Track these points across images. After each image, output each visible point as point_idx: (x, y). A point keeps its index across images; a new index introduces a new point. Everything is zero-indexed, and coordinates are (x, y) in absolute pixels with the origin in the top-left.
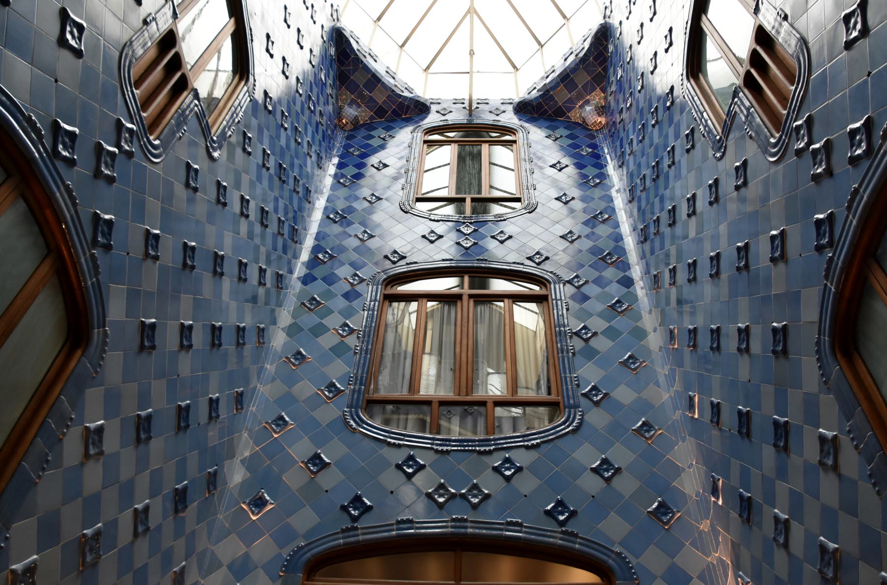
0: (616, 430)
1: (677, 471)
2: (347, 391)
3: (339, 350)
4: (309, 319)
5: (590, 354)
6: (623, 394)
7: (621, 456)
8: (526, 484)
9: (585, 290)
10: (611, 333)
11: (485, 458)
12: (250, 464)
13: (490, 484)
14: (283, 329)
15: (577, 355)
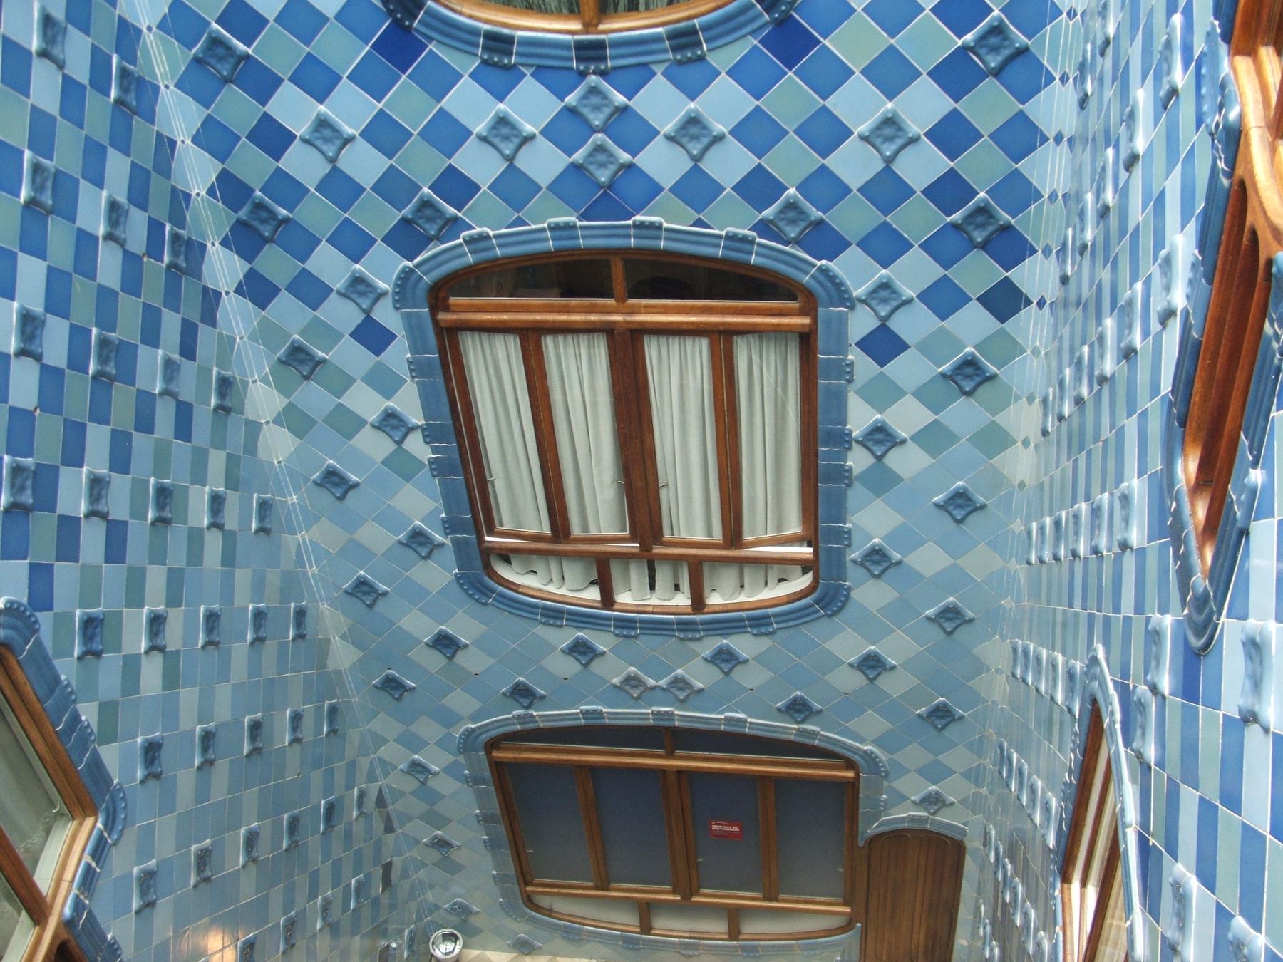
0: (899, 613)
1: (979, 667)
2: (448, 542)
3: (401, 465)
4: (314, 397)
5: (882, 481)
6: (928, 559)
7: (895, 648)
8: (751, 677)
9: (902, 325)
10: (933, 438)
11: (694, 646)
12: (352, 637)
13: (700, 675)
14: (277, 421)
15: (856, 483)
